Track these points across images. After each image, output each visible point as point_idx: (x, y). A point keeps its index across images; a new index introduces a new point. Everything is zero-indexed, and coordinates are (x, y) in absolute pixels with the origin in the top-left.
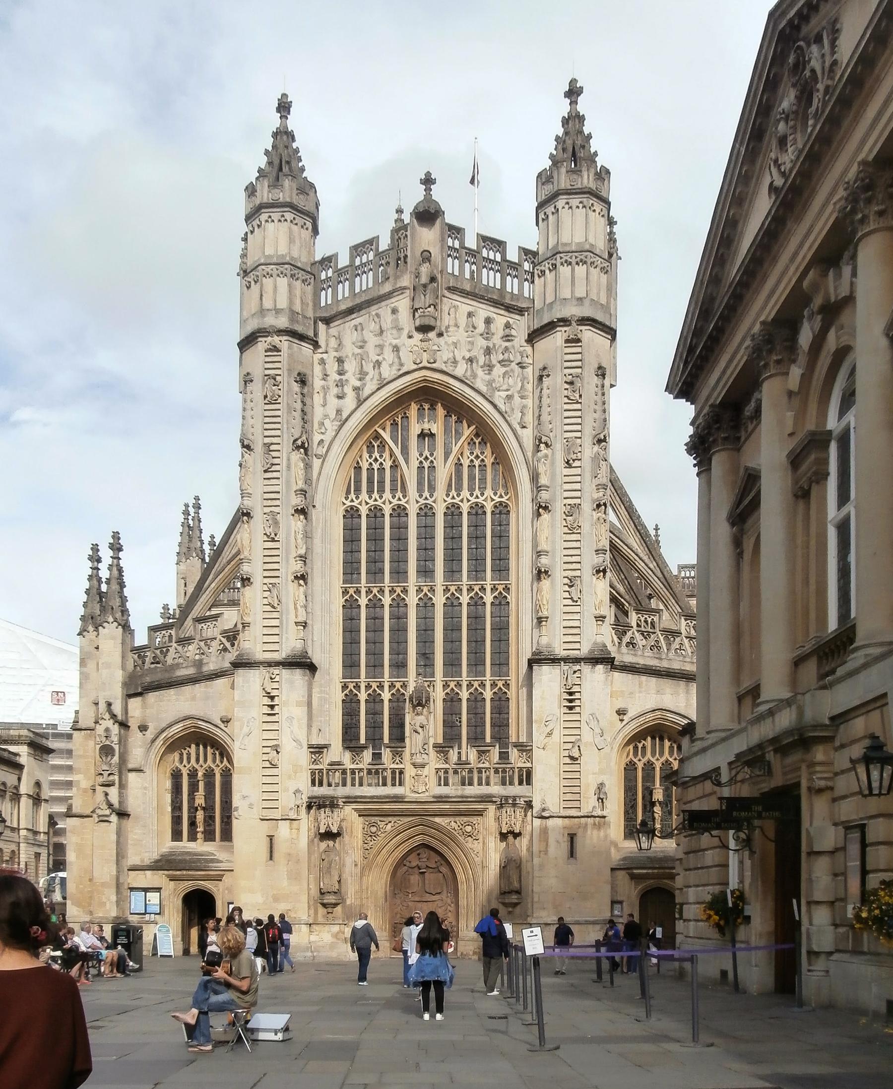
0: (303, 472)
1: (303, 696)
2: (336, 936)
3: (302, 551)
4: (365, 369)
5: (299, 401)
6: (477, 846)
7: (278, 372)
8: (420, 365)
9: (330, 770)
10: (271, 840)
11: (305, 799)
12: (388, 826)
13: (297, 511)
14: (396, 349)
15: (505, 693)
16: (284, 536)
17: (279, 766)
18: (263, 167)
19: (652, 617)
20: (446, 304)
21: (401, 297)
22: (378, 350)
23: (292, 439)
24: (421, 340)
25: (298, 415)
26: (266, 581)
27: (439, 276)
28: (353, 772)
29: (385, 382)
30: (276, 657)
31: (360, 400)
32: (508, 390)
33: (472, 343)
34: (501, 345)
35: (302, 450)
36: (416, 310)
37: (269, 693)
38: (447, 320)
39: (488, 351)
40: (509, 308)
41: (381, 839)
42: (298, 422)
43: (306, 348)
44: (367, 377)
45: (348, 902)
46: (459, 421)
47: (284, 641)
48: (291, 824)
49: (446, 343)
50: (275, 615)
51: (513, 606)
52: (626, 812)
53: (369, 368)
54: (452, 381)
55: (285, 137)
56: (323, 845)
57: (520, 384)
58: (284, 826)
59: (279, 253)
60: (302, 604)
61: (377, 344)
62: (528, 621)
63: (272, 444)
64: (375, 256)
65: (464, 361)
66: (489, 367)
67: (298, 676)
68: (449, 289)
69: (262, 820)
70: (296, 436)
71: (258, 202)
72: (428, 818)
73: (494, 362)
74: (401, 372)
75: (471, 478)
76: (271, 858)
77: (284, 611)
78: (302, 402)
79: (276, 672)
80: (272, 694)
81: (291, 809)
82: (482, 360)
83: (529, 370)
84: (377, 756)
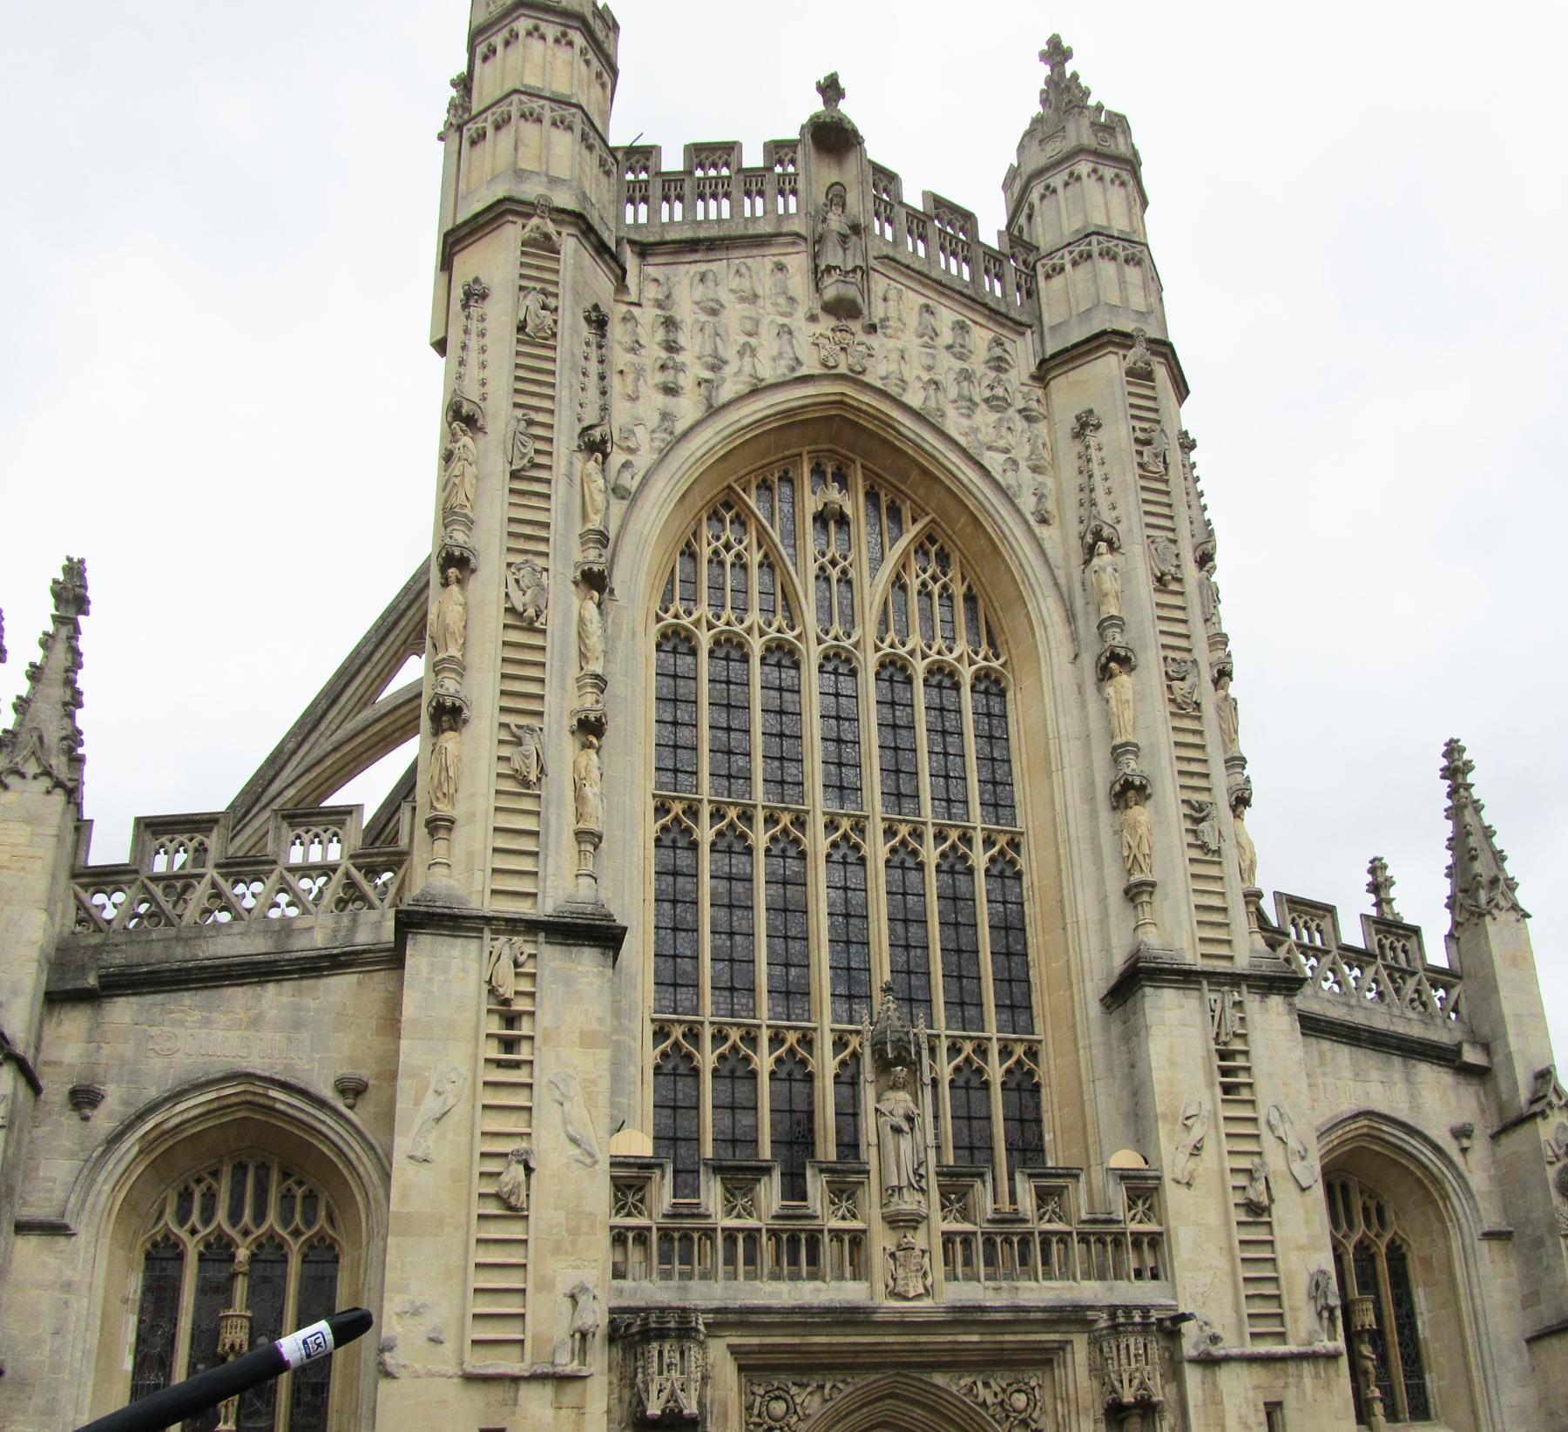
1: (600, 1020)
3: (596, 667)
4: (722, 352)
8: (832, 372)
14: (786, 331)
20: (879, 284)
21: (790, 250)
26: (512, 720)
28: (730, 1235)
29: (764, 384)
31: (710, 406)
37: (506, 1002)
47: (551, 869)
49: (882, 346)
53: (730, 353)
60: (596, 789)
61: (747, 314)
69: (470, 1379)
80: (515, 1007)
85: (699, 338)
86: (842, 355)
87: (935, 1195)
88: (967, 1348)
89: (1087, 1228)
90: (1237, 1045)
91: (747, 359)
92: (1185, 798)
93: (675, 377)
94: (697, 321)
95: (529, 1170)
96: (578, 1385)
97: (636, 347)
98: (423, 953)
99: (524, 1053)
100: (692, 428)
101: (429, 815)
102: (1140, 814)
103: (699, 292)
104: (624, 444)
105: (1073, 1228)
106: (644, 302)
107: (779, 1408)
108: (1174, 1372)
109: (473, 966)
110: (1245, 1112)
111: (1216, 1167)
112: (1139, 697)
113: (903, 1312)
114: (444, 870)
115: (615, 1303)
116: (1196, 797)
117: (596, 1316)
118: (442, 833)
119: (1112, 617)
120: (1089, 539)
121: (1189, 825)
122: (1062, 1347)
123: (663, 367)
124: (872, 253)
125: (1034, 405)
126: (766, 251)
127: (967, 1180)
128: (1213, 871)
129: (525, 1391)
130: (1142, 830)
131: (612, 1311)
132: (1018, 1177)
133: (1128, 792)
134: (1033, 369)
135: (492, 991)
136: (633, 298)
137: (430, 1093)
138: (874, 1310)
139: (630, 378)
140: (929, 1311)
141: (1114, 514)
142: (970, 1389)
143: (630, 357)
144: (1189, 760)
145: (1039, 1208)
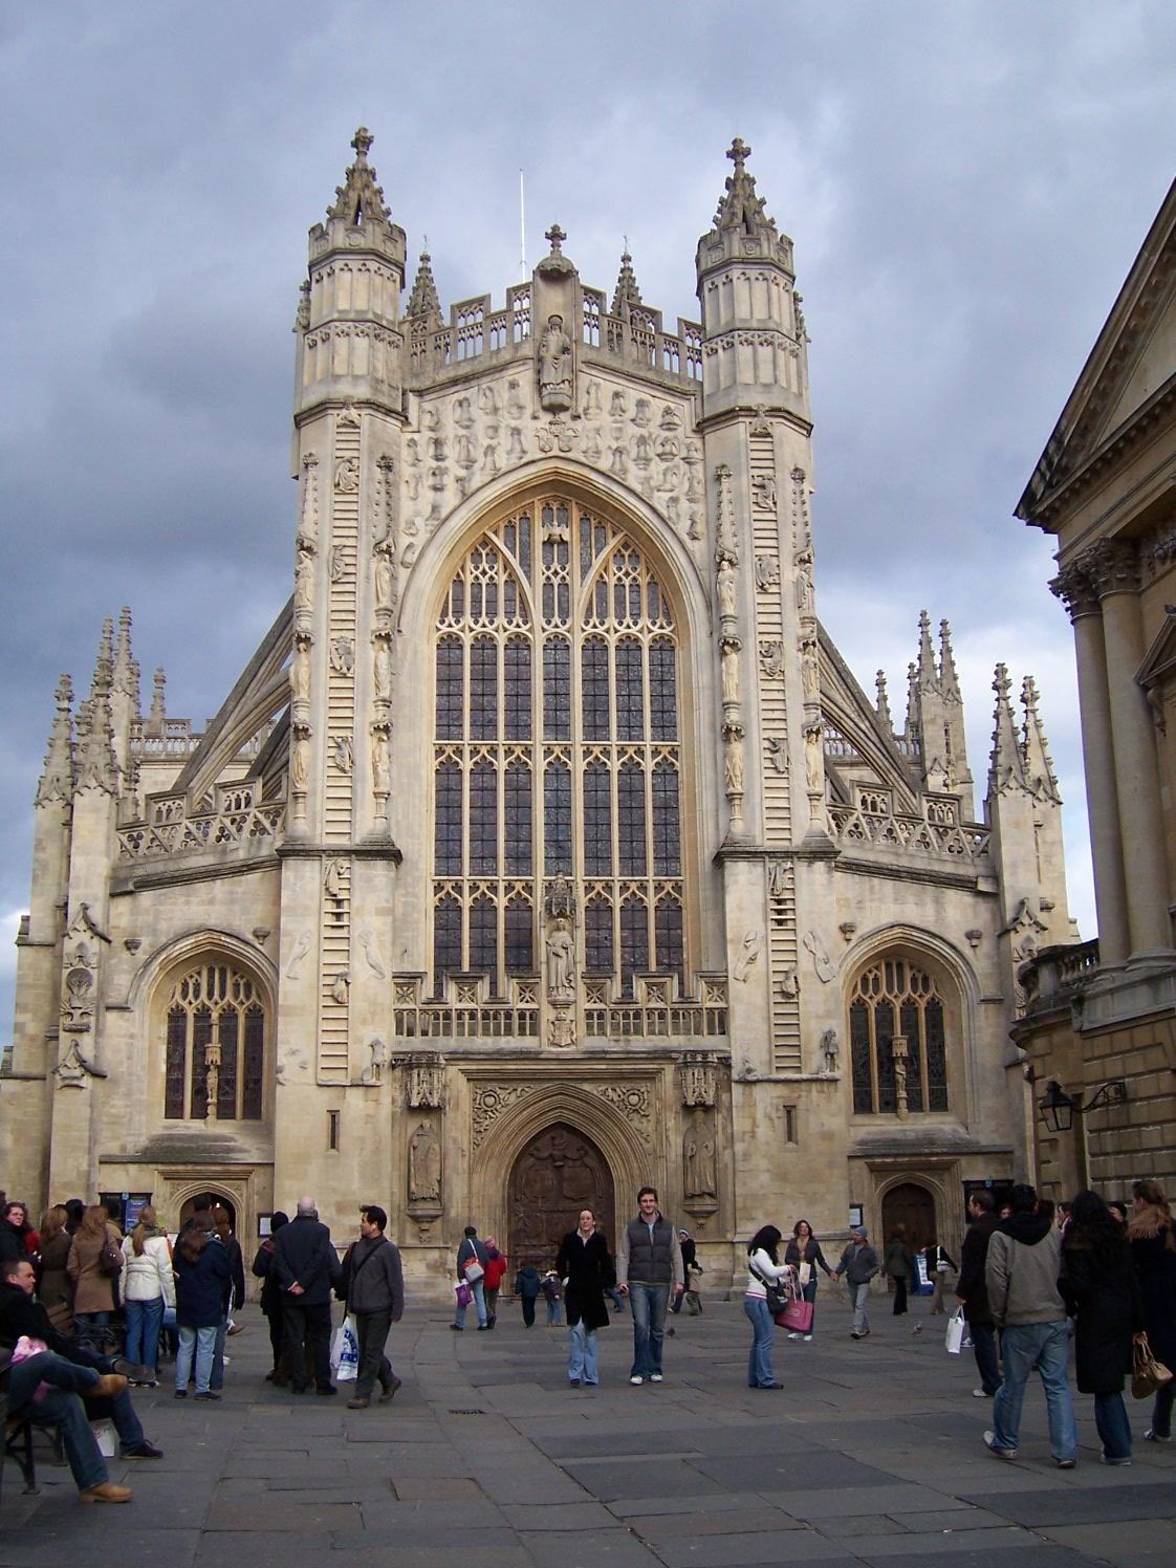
1: (387, 901)
3: (385, 694)
6: (648, 1126)
7: (355, 454)
9: (425, 1011)
10: (333, 1117)
12: (510, 1097)
13: (379, 637)
15: (676, 899)
18: (334, 206)
20: (584, 380)
21: (521, 368)
22: (490, 431)
23: (373, 542)
24: (551, 423)
25: (382, 509)
29: (501, 472)
32: (672, 491)
34: (659, 435)
35: (387, 556)
36: (545, 385)
39: (642, 441)
40: (670, 391)
41: (498, 1119)
42: (382, 520)
43: (393, 425)
44: (476, 465)
45: (453, 1213)
46: (600, 527)
48: (366, 1094)
50: (346, 782)
51: (683, 777)
53: (478, 454)
54: (593, 476)
55: (364, 175)
56: (413, 1125)
57: (687, 485)
58: (355, 1097)
59: (358, 308)
62: (707, 801)
64: (486, 318)
65: (610, 452)
66: (648, 460)
67: (380, 870)
68: (588, 363)
70: (378, 538)
71: (330, 248)
73: (652, 455)
75: (620, 601)
76: (333, 1144)
79: (346, 864)
80: (339, 897)
83: (699, 468)
84: (494, 984)
85: (457, 447)
86: (556, 440)
87: (582, 989)
88: (599, 1071)
89: (677, 1006)
91: (489, 459)
94: (456, 436)
95: (347, 983)
96: (375, 1089)
98: (292, 870)
100: (452, 513)
102: (737, 748)
106: (422, 429)
107: (490, 1101)
108: (725, 1084)
109: (317, 875)
111: (764, 970)
112: (743, 668)
113: (560, 1053)
115: (394, 1050)
116: (772, 735)
117: (385, 1056)
122: (660, 1071)
123: (434, 474)
124: (580, 359)
125: (694, 454)
126: (504, 373)
127: (602, 981)
128: (783, 784)
129: (348, 1090)
130: (737, 760)
133: (729, 734)
135: (327, 889)
136: (415, 428)
137: (297, 944)
138: (541, 1053)
139: (412, 485)
140: (573, 1053)
142: (604, 1093)
143: (411, 470)
145: (649, 993)
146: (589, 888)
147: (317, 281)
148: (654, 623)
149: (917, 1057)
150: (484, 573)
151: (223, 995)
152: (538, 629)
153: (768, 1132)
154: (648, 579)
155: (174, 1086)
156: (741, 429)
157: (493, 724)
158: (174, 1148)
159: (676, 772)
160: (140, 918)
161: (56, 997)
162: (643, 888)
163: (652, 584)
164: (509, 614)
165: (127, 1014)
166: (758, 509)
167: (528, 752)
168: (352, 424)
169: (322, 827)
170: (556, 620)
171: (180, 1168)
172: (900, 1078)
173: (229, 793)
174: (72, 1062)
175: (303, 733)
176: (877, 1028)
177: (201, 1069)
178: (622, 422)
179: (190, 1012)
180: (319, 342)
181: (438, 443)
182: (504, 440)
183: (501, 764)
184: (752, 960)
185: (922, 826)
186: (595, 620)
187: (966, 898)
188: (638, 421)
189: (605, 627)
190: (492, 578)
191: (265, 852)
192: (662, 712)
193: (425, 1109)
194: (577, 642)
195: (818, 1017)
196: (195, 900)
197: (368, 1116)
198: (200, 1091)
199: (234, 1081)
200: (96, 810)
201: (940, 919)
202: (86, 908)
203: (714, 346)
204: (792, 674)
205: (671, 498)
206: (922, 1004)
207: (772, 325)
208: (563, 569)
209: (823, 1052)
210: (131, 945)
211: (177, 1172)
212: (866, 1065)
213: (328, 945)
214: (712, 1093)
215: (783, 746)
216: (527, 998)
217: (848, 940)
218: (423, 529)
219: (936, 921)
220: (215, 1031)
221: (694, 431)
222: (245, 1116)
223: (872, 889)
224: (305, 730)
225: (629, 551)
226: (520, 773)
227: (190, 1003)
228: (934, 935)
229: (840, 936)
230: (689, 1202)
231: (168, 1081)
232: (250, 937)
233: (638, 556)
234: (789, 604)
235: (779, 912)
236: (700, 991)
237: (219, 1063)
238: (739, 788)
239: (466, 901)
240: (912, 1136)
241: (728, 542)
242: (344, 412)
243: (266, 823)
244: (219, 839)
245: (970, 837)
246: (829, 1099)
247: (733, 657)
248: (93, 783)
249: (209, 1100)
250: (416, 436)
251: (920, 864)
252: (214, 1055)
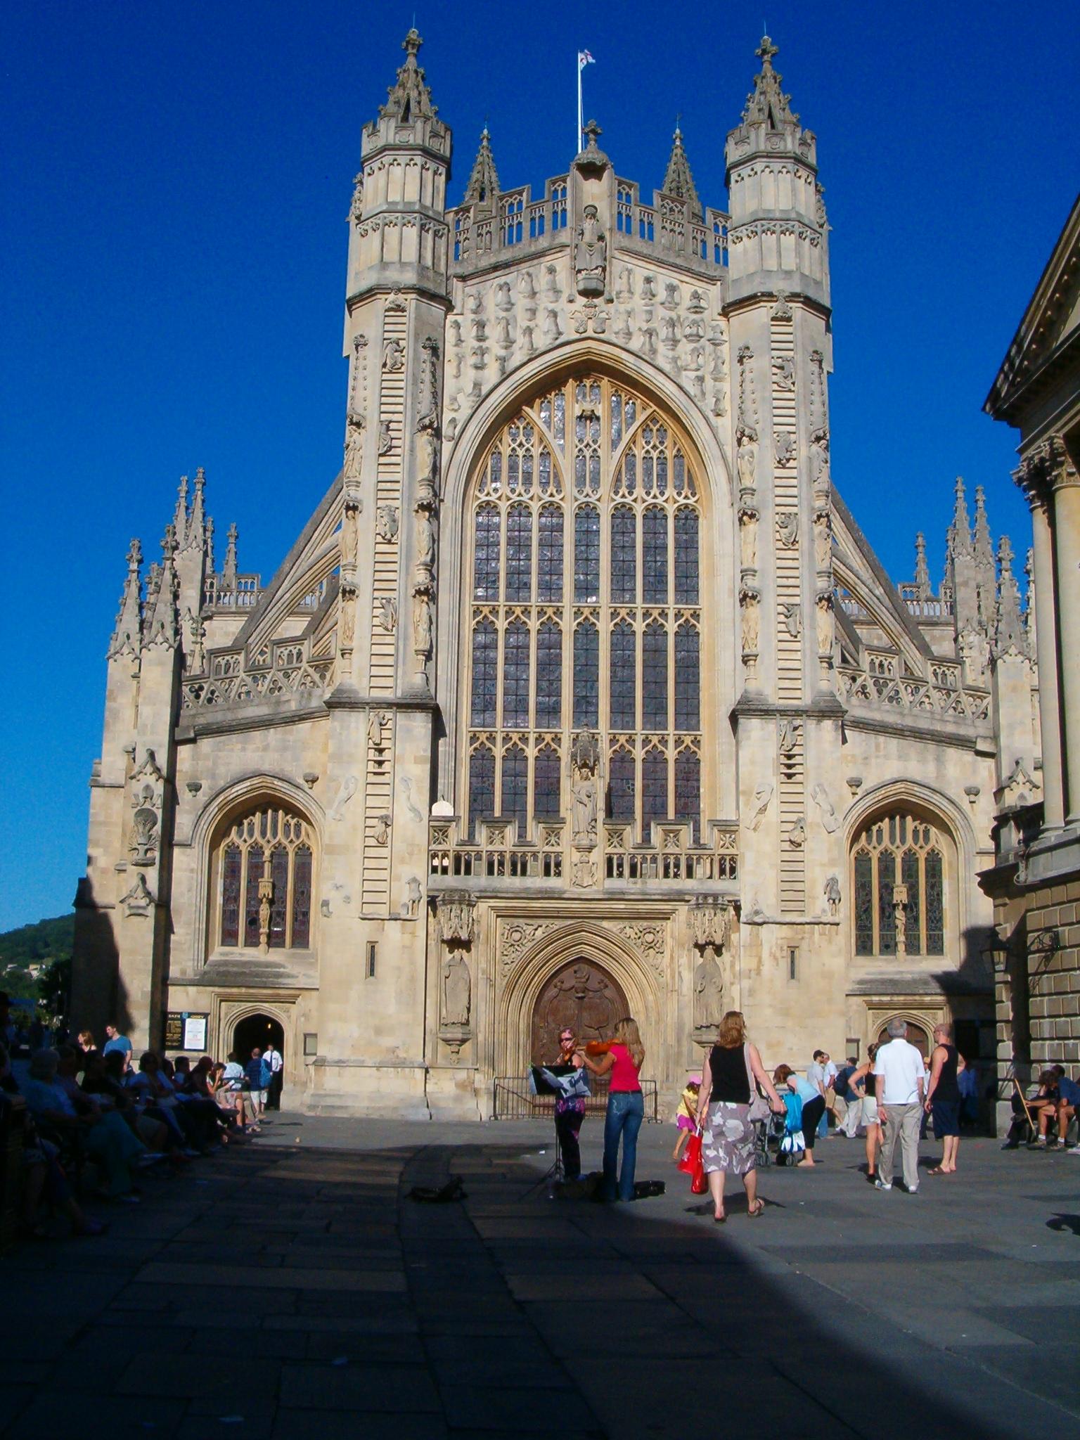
0: (432, 456)
1: (425, 751)
2: (461, 1086)
5: (428, 372)
8: (584, 335)
11: (423, 889)
14: (554, 314)
16: (404, 537)
17: (389, 844)
19: (889, 660)
21: (559, 255)
22: (528, 315)
24: (585, 306)
25: (427, 388)
26: (377, 594)
27: (607, 235)
29: (538, 352)
30: (388, 695)
32: (697, 370)
33: (650, 312)
35: (429, 430)
38: (616, 284)
39: (672, 324)
42: (426, 396)
43: (437, 310)
45: (481, 1037)
48: (403, 925)
50: (389, 640)
51: (703, 639)
52: (858, 917)
54: (624, 355)
57: (713, 364)
58: (393, 928)
63: (390, 422)
66: (675, 342)
70: (424, 412)
72: (593, 921)
73: (679, 336)
74: (558, 342)
76: (372, 972)
77: (401, 636)
78: (432, 372)
79: (389, 715)
80: (381, 747)
81: (405, 905)
82: (664, 332)
89: (691, 852)
90: (796, 751)
92: (780, 602)
93: (482, 359)
97: (460, 341)
99: (386, 767)
101: (340, 646)
102: (754, 611)
103: (501, 296)
104: (451, 407)
105: (684, 852)
107: (516, 936)
110: (798, 788)
114: (348, 675)
118: (347, 656)
119: (744, 489)
120: (739, 433)
121: (782, 618)
122: (674, 911)
127: (623, 827)
130: (752, 623)
131: (428, 890)
132: (652, 825)
133: (746, 598)
134: (720, 311)
138: (565, 892)
139: (455, 364)
141: (756, 417)
144: (787, 577)
146: (613, 741)
147: (369, 175)
148: (679, 494)
149: (917, 904)
150: (521, 445)
151: (275, 834)
152: (568, 498)
153: (774, 971)
154: (675, 452)
155: (230, 916)
156: (761, 314)
157: (527, 586)
158: (229, 972)
159: (698, 634)
160: (200, 763)
161: (124, 834)
162: (663, 741)
163: (679, 456)
164: (544, 485)
165: (188, 850)
166: (775, 387)
167: (558, 612)
168: (399, 308)
169: (365, 682)
170: (588, 490)
171: (235, 990)
172: (898, 922)
173: (282, 649)
174: (140, 893)
175: (350, 593)
176: (880, 876)
177: (254, 900)
178: (652, 305)
179: (244, 849)
180: (370, 231)
181: (481, 325)
182: (543, 322)
183: (534, 624)
184: (763, 810)
185: (925, 689)
186: (624, 490)
187: (969, 756)
188: (667, 305)
189: (634, 497)
190: (528, 450)
191: (315, 703)
192: (687, 577)
193: (455, 943)
194: (605, 511)
195: (823, 865)
196: (251, 747)
197: (404, 947)
198: (253, 921)
199: (284, 913)
200: (161, 663)
201: (940, 775)
202: (152, 755)
203: (739, 235)
204: (803, 542)
205: (697, 377)
206: (922, 856)
207: (793, 215)
208: (595, 442)
209: (826, 897)
210: (195, 788)
211: (231, 994)
212: (868, 911)
213: (371, 789)
214: (720, 934)
215: (796, 610)
216: (553, 842)
217: (854, 794)
218: (466, 405)
219: (937, 778)
220: (267, 867)
221: (720, 315)
222: (293, 945)
223: (877, 746)
224: (352, 592)
225: (658, 426)
226: (550, 630)
227: (245, 841)
228: (934, 791)
229: (847, 790)
230: (698, 1032)
231: (224, 912)
232: (301, 781)
233: (665, 430)
234: (805, 478)
235: (789, 766)
236: (709, 836)
237: (270, 896)
238: (754, 651)
239: (499, 751)
240: (909, 977)
241: (750, 419)
242: (392, 297)
243: (316, 677)
244: (271, 690)
245: (971, 699)
246: (830, 941)
247: (752, 527)
248: (160, 639)
249: (262, 930)
250: (459, 318)
251: (923, 724)
252: (265, 889)
